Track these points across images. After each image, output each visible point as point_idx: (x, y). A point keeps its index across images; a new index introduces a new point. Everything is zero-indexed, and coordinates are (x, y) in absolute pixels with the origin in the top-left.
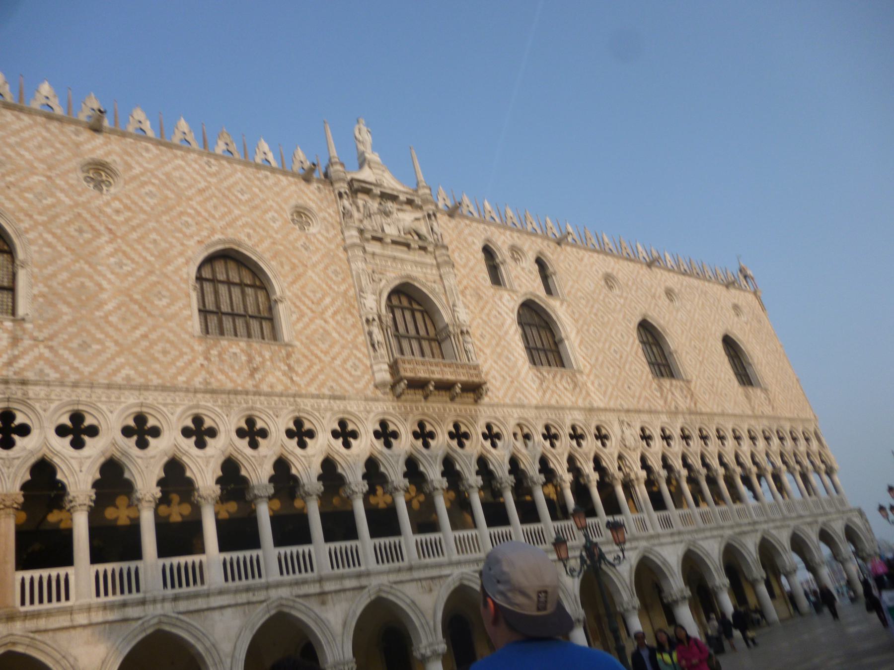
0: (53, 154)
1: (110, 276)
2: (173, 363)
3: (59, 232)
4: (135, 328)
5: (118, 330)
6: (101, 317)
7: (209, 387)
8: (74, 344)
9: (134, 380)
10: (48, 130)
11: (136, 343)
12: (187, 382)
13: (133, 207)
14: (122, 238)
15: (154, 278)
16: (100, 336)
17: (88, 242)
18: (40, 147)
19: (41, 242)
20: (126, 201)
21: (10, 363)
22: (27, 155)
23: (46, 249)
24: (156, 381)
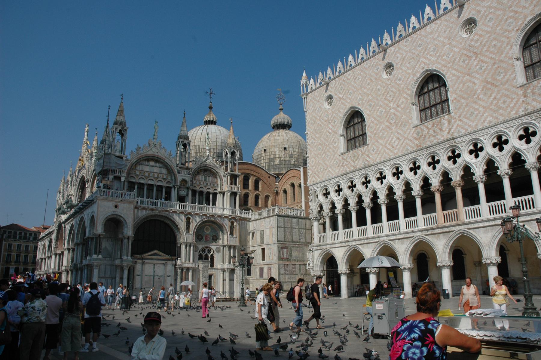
0: (449, 31)
1: (478, 76)
2: (508, 106)
3: (456, 67)
4: (490, 96)
5: (484, 100)
6: (476, 98)
7: (527, 112)
8: (468, 115)
9: (492, 122)
10: (446, 21)
11: (491, 103)
13: (483, 33)
14: (480, 54)
15: (496, 66)
16: (477, 107)
17: (467, 65)
18: (445, 32)
19: (451, 76)
20: (480, 32)
21: (449, 132)
22: (441, 39)
23: (453, 78)
24: (501, 119)
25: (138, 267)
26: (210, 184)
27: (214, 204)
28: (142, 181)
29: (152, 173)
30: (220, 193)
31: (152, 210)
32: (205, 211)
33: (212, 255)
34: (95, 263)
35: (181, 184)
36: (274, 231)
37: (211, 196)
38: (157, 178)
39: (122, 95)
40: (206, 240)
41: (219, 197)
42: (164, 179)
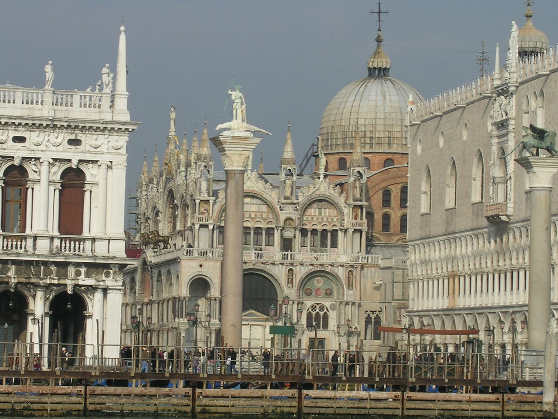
26: (327, 219)
27: (334, 245)
36: (391, 285)
37: (329, 234)
38: (255, 218)
40: (317, 294)
41: (340, 234)
42: (263, 219)
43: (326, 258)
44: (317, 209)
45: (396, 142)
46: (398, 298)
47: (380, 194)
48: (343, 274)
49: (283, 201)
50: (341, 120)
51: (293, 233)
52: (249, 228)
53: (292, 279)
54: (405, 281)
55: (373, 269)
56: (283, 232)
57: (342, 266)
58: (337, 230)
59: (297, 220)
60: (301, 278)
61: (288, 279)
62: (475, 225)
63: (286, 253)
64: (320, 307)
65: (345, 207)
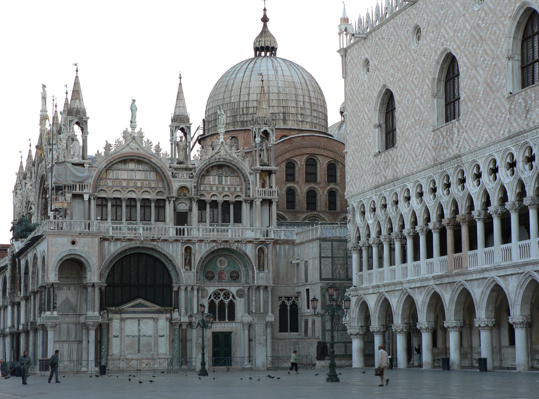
12: (503, 134)
21: (457, 147)
23: (465, 68)
25: (115, 325)
26: (229, 188)
27: (238, 219)
28: (117, 195)
29: (132, 181)
30: (246, 201)
31: (130, 240)
32: (214, 235)
33: (231, 301)
34: (49, 323)
35: (179, 195)
36: (317, 261)
37: (232, 207)
38: (141, 188)
39: (76, 65)
40: (221, 279)
41: (245, 207)
42: (151, 188)
43: (231, 232)
44: (217, 177)
45: (291, 119)
46: (326, 277)
47: (284, 165)
48: (251, 253)
49: (175, 165)
50: (231, 97)
51: (189, 205)
52: (134, 200)
53: (190, 260)
54: (335, 256)
55: (287, 247)
56: (177, 203)
57: (250, 242)
58: (240, 203)
59: (193, 190)
60: (201, 258)
61: (185, 260)
62: (518, 129)
63: (182, 227)
64: (224, 294)
65: (250, 174)
